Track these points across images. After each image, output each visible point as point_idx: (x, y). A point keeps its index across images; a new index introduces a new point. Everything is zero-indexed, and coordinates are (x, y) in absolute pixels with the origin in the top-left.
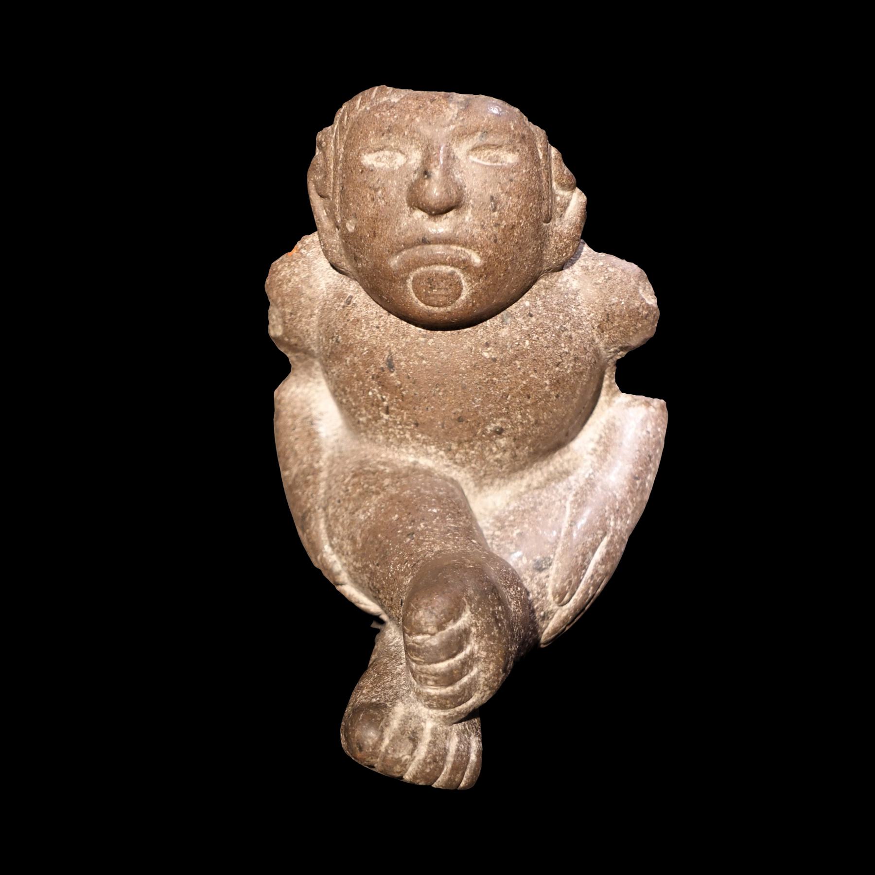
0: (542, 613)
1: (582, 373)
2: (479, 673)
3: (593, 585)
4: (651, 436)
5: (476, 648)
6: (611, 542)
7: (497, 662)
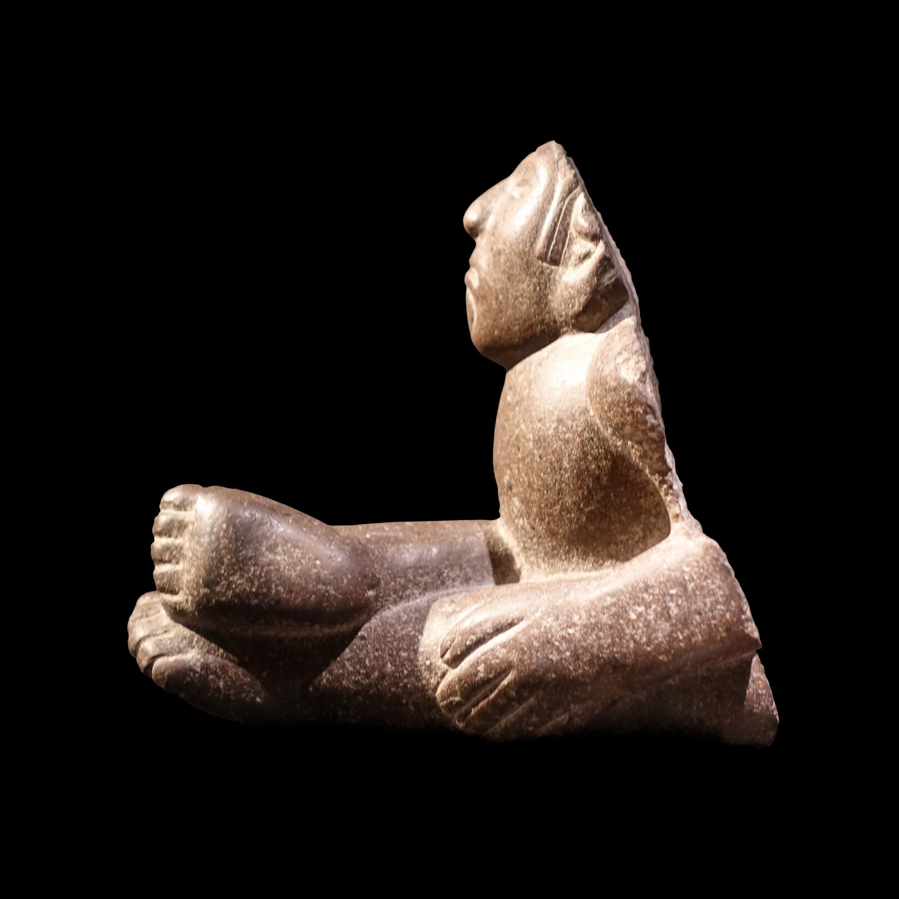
0: (428, 663)
1: (567, 442)
2: (183, 570)
3: (485, 662)
4: (665, 567)
5: (187, 545)
6: (524, 631)
7: (198, 569)
